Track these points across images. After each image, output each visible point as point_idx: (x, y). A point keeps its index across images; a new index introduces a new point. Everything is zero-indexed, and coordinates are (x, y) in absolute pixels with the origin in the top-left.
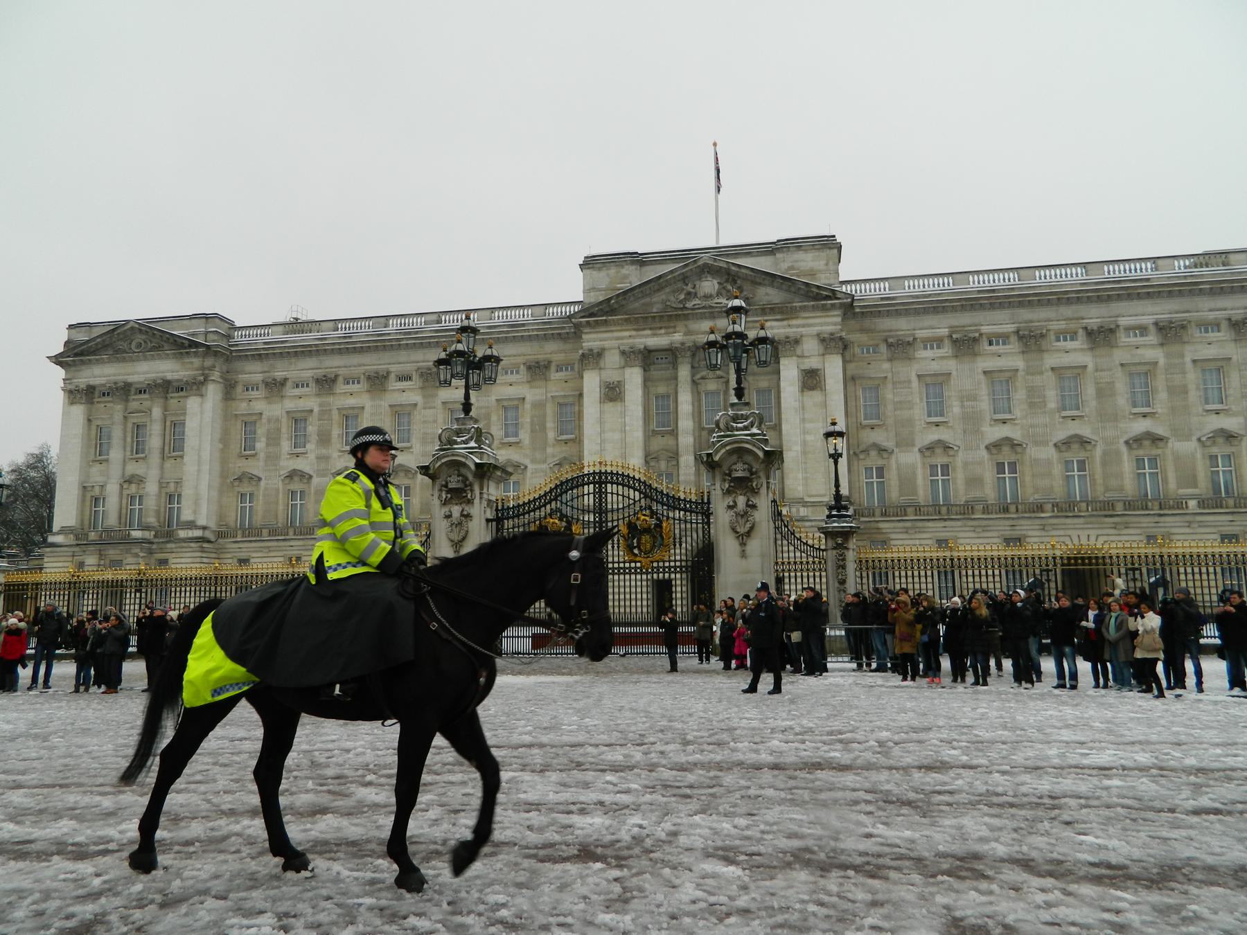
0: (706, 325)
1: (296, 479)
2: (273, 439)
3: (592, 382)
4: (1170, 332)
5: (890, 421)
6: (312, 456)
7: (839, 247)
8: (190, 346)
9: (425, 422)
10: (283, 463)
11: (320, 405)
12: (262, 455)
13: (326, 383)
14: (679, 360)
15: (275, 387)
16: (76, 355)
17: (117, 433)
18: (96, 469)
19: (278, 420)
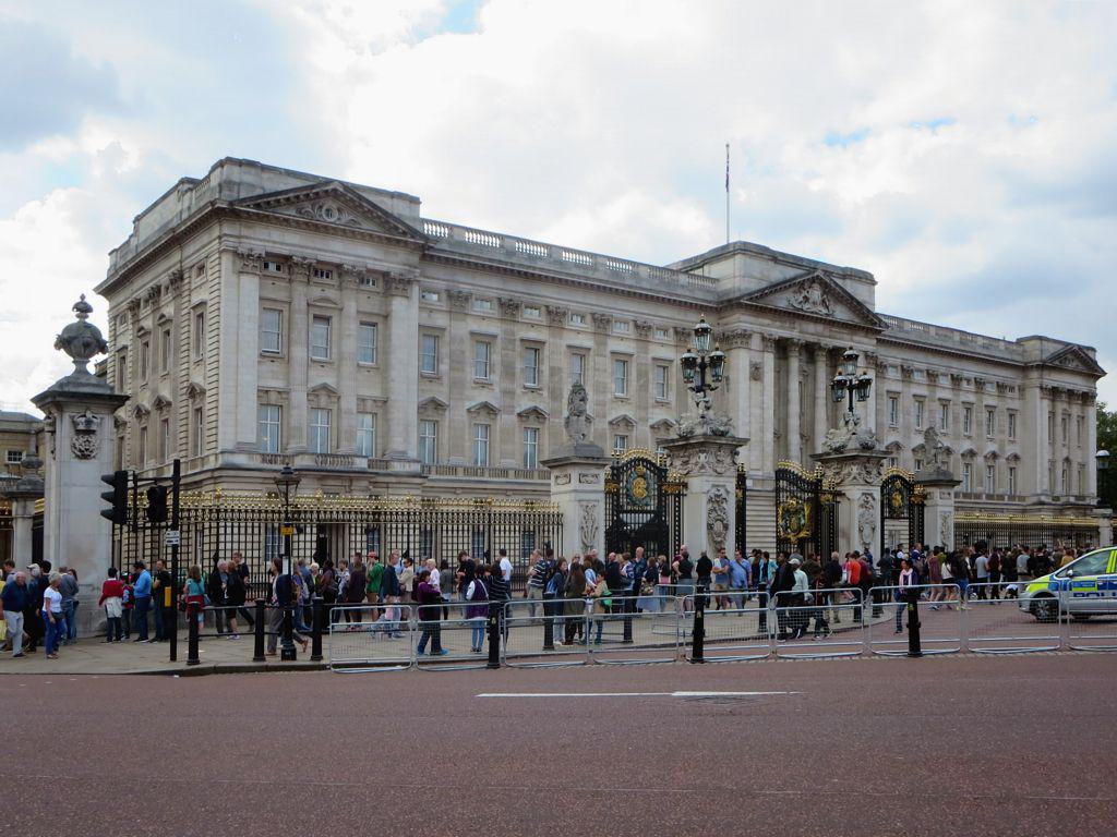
0: (811, 327)
1: (483, 412)
2: (457, 363)
4: (980, 384)
6: (497, 389)
7: (873, 283)
8: (404, 233)
9: (598, 370)
10: (467, 393)
11: (506, 332)
14: (791, 354)
15: (458, 301)
16: (258, 206)
18: (268, 366)
19: (462, 340)
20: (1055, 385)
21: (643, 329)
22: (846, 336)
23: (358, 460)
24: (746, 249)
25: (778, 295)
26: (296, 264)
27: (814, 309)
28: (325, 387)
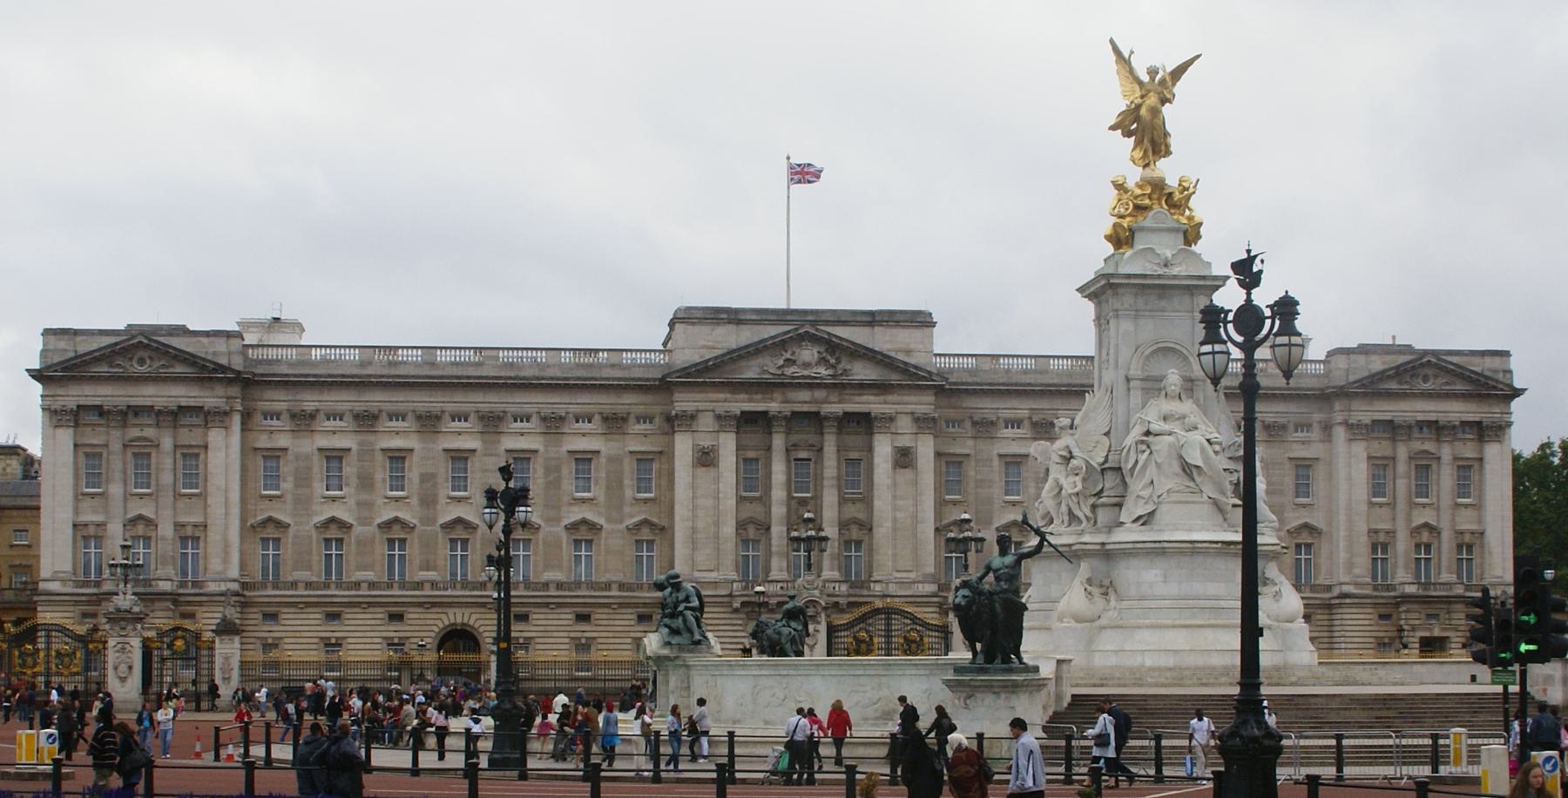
0: (804, 395)
1: (333, 527)
2: (303, 480)
3: (683, 446)
5: (971, 498)
6: (352, 502)
7: (933, 325)
10: (316, 508)
11: (360, 444)
12: (289, 497)
13: (366, 420)
15: (303, 421)
16: (64, 369)
17: (117, 464)
18: (86, 504)
19: (308, 457)
20: (1388, 416)
21: (553, 424)
22: (872, 398)
23: (161, 583)
24: (684, 318)
25: (743, 363)
26: (109, 412)
27: (806, 373)
28: (140, 517)
